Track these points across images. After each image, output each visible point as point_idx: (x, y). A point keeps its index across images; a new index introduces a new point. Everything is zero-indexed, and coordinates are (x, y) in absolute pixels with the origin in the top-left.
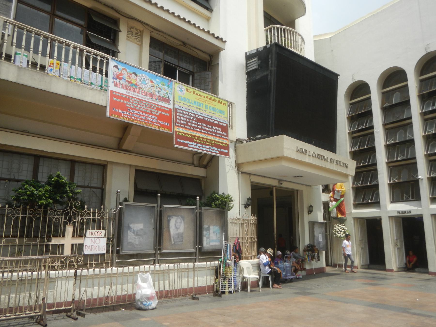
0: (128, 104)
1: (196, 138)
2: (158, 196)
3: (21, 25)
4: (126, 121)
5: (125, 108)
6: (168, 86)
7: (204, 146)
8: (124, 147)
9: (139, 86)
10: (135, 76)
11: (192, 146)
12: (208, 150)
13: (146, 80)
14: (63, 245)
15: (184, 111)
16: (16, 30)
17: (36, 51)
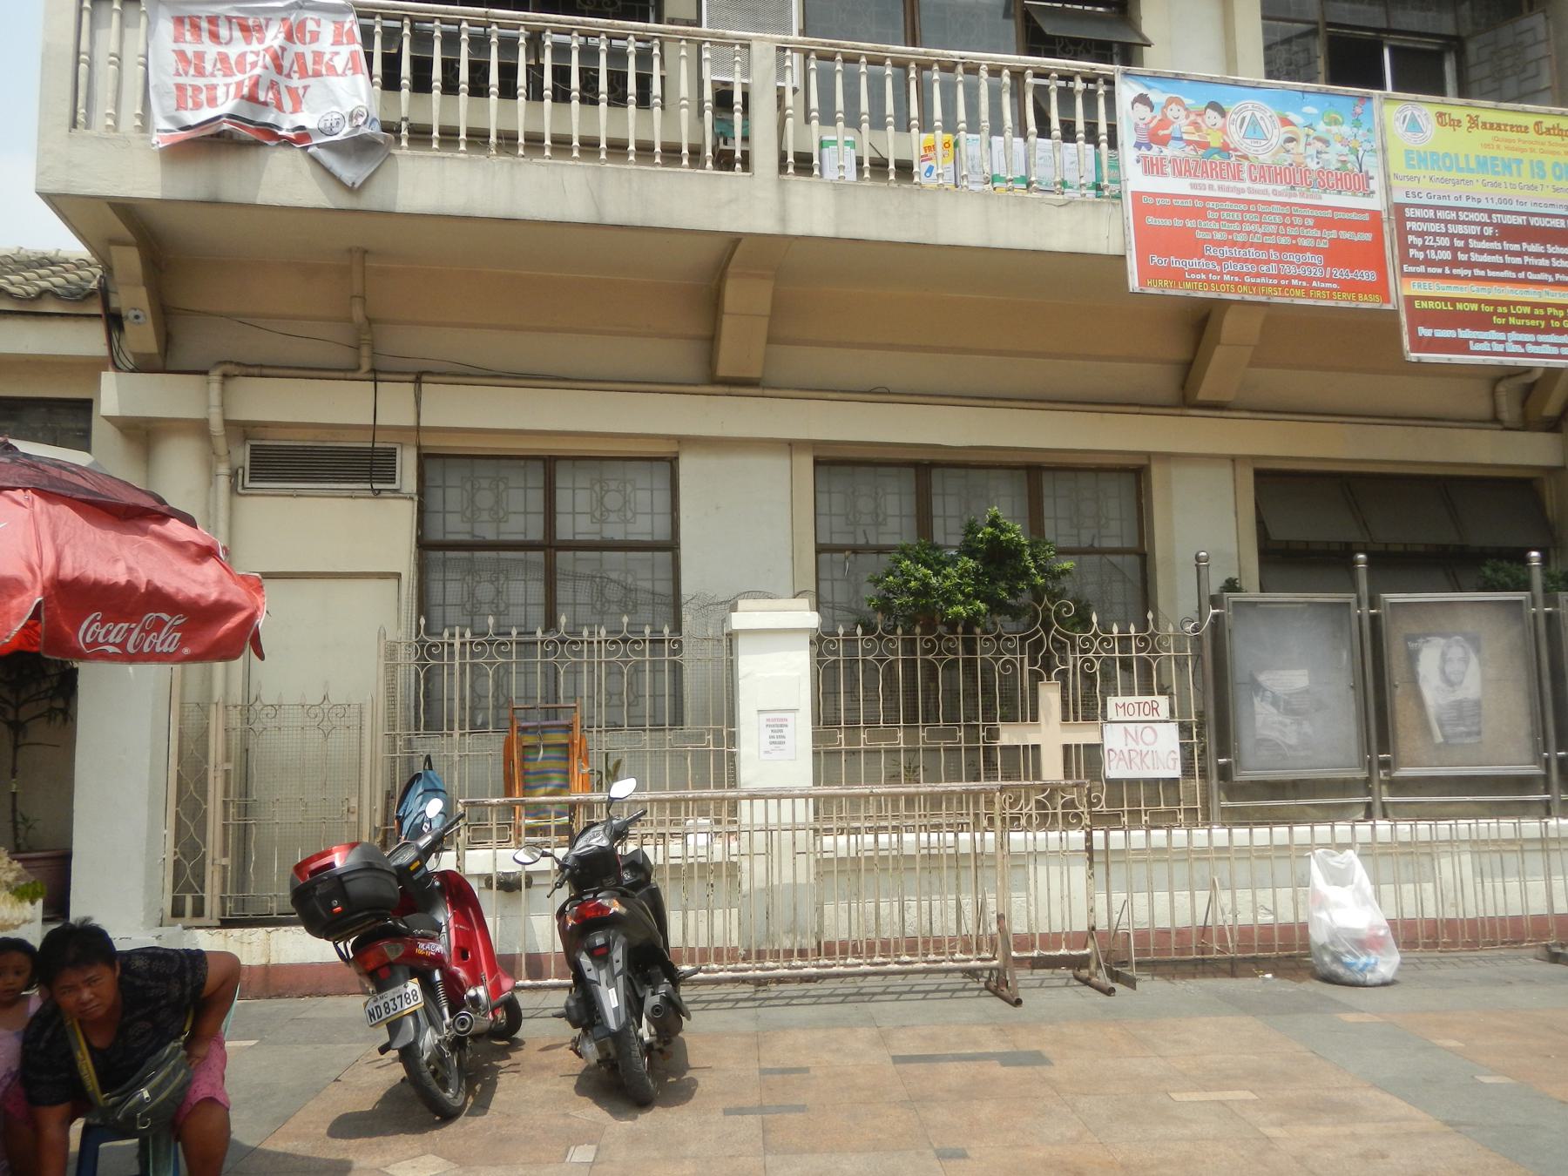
0: (1201, 229)
1: (1500, 310)
2: (1356, 562)
3: (824, 45)
4: (1200, 294)
5: (1192, 247)
6: (1357, 124)
7: (1541, 338)
8: (1203, 395)
9: (1235, 150)
10: (1218, 117)
11: (1485, 347)
13: (1262, 123)
14: (1036, 748)
15: (1436, 208)
16: (813, 65)
17: (878, 123)
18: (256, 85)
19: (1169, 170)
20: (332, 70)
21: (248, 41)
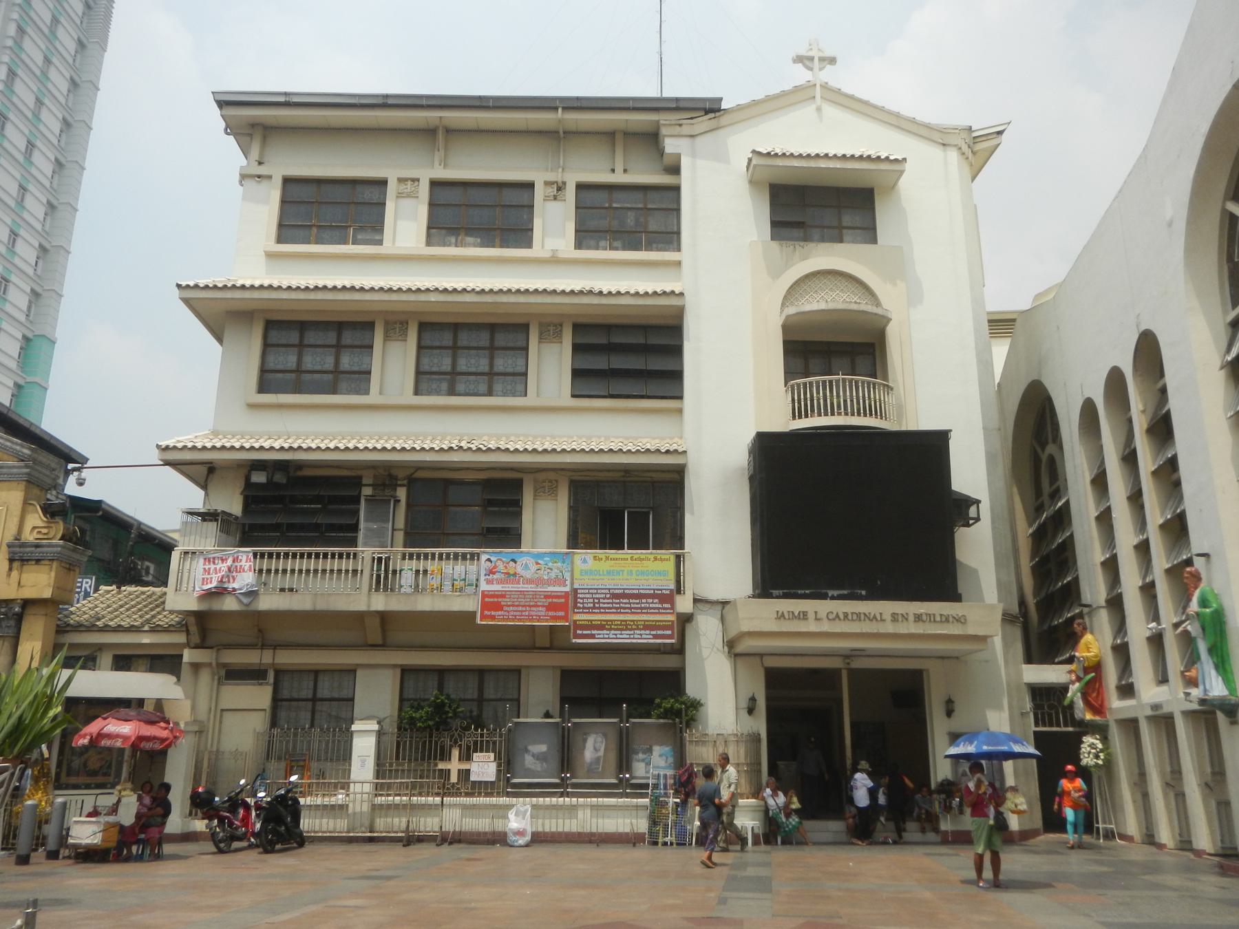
7: (623, 632)
12: (632, 636)
14: (449, 770)
18: (222, 577)
20: (244, 571)
21: (223, 563)
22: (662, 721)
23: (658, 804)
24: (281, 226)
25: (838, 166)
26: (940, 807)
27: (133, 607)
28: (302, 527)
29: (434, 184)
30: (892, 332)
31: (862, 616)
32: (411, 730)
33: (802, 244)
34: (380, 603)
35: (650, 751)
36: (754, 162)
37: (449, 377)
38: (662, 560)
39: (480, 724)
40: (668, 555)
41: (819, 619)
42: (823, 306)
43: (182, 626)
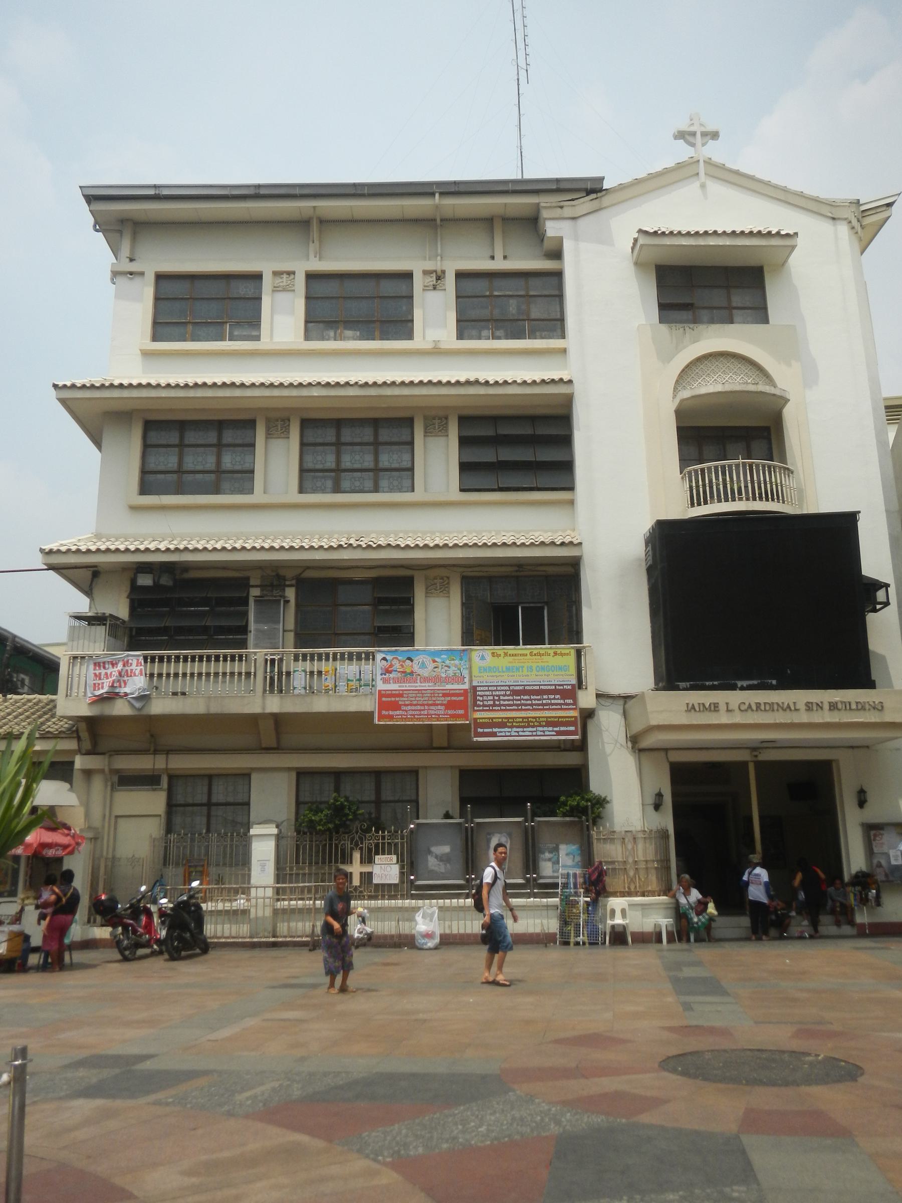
1: (510, 720)
6: (461, 659)
7: (525, 729)
11: (503, 734)
12: (534, 733)
18: (113, 682)
19: (391, 682)
22: (568, 819)
23: (569, 904)
24: (156, 323)
25: (728, 244)
26: (855, 900)
27: (21, 714)
28: (190, 630)
29: (311, 277)
30: (789, 413)
31: (776, 707)
32: (311, 834)
33: (692, 326)
34: (274, 705)
35: (556, 850)
36: (641, 241)
37: (333, 474)
38: (562, 654)
39: (380, 827)
40: (568, 649)
41: (731, 711)
42: (719, 388)
43: (73, 732)
